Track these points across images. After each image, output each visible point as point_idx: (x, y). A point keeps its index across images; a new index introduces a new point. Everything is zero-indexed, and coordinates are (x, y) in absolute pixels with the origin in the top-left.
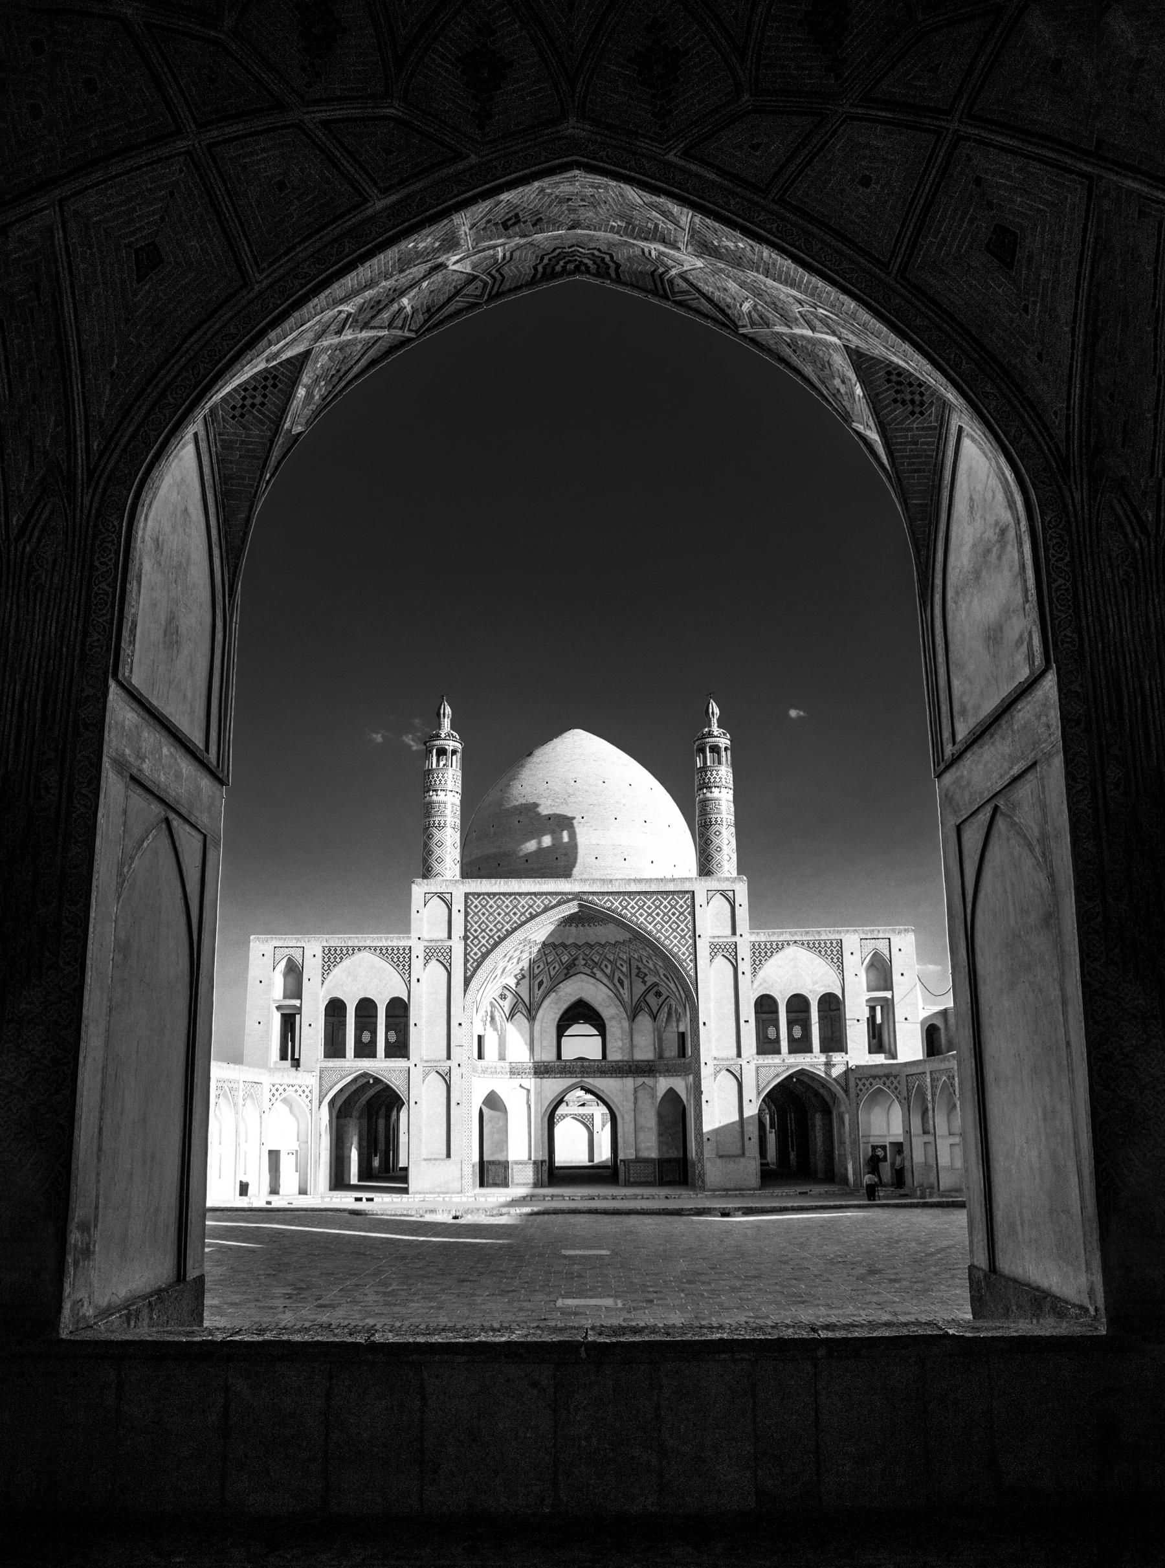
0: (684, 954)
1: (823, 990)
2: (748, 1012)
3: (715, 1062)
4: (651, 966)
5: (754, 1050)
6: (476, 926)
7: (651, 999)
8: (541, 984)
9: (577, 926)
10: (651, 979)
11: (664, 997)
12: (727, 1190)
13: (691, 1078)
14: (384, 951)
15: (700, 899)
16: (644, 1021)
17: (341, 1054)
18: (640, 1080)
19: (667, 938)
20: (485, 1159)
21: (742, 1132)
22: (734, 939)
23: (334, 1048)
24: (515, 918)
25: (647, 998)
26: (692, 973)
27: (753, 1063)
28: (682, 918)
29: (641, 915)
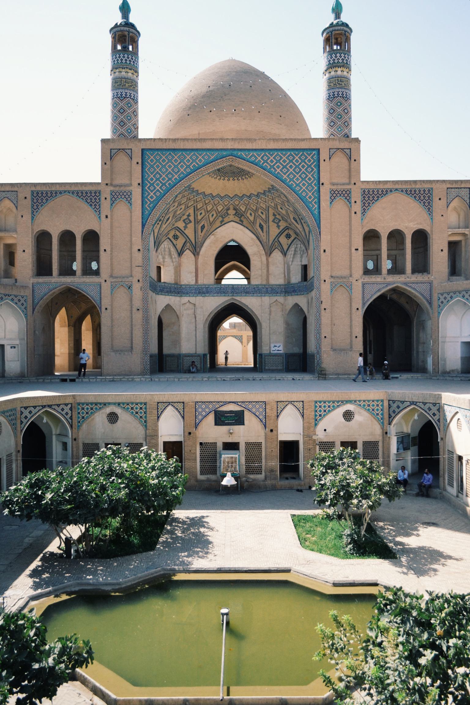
0: (310, 197)
1: (415, 227)
2: (358, 242)
3: (332, 280)
4: (284, 212)
5: (361, 272)
6: (152, 176)
7: (283, 240)
8: (203, 227)
9: (229, 180)
10: (283, 225)
11: (292, 238)
12: (338, 374)
13: (313, 293)
14: (80, 194)
15: (324, 155)
16: (277, 255)
17: (49, 273)
18: (275, 298)
19: (298, 185)
20: (166, 351)
21: (351, 332)
22: (348, 187)
23: (43, 268)
24: (182, 170)
25: (280, 239)
26: (316, 212)
27: (360, 282)
28: (309, 170)
29: (278, 167)
